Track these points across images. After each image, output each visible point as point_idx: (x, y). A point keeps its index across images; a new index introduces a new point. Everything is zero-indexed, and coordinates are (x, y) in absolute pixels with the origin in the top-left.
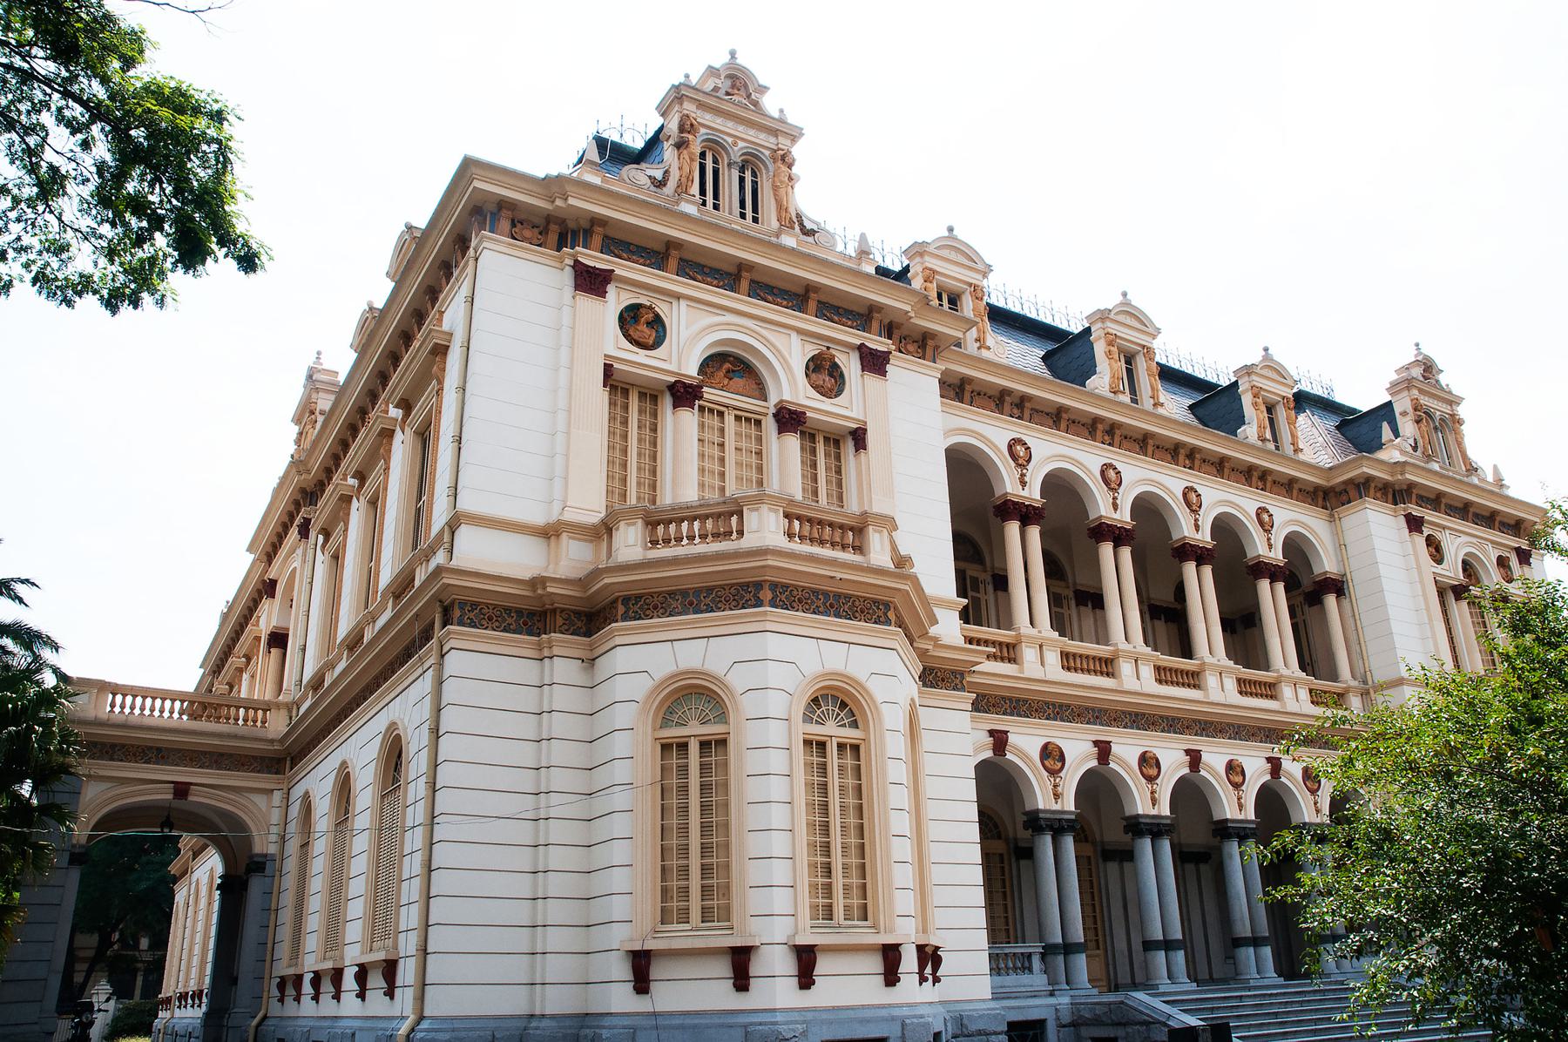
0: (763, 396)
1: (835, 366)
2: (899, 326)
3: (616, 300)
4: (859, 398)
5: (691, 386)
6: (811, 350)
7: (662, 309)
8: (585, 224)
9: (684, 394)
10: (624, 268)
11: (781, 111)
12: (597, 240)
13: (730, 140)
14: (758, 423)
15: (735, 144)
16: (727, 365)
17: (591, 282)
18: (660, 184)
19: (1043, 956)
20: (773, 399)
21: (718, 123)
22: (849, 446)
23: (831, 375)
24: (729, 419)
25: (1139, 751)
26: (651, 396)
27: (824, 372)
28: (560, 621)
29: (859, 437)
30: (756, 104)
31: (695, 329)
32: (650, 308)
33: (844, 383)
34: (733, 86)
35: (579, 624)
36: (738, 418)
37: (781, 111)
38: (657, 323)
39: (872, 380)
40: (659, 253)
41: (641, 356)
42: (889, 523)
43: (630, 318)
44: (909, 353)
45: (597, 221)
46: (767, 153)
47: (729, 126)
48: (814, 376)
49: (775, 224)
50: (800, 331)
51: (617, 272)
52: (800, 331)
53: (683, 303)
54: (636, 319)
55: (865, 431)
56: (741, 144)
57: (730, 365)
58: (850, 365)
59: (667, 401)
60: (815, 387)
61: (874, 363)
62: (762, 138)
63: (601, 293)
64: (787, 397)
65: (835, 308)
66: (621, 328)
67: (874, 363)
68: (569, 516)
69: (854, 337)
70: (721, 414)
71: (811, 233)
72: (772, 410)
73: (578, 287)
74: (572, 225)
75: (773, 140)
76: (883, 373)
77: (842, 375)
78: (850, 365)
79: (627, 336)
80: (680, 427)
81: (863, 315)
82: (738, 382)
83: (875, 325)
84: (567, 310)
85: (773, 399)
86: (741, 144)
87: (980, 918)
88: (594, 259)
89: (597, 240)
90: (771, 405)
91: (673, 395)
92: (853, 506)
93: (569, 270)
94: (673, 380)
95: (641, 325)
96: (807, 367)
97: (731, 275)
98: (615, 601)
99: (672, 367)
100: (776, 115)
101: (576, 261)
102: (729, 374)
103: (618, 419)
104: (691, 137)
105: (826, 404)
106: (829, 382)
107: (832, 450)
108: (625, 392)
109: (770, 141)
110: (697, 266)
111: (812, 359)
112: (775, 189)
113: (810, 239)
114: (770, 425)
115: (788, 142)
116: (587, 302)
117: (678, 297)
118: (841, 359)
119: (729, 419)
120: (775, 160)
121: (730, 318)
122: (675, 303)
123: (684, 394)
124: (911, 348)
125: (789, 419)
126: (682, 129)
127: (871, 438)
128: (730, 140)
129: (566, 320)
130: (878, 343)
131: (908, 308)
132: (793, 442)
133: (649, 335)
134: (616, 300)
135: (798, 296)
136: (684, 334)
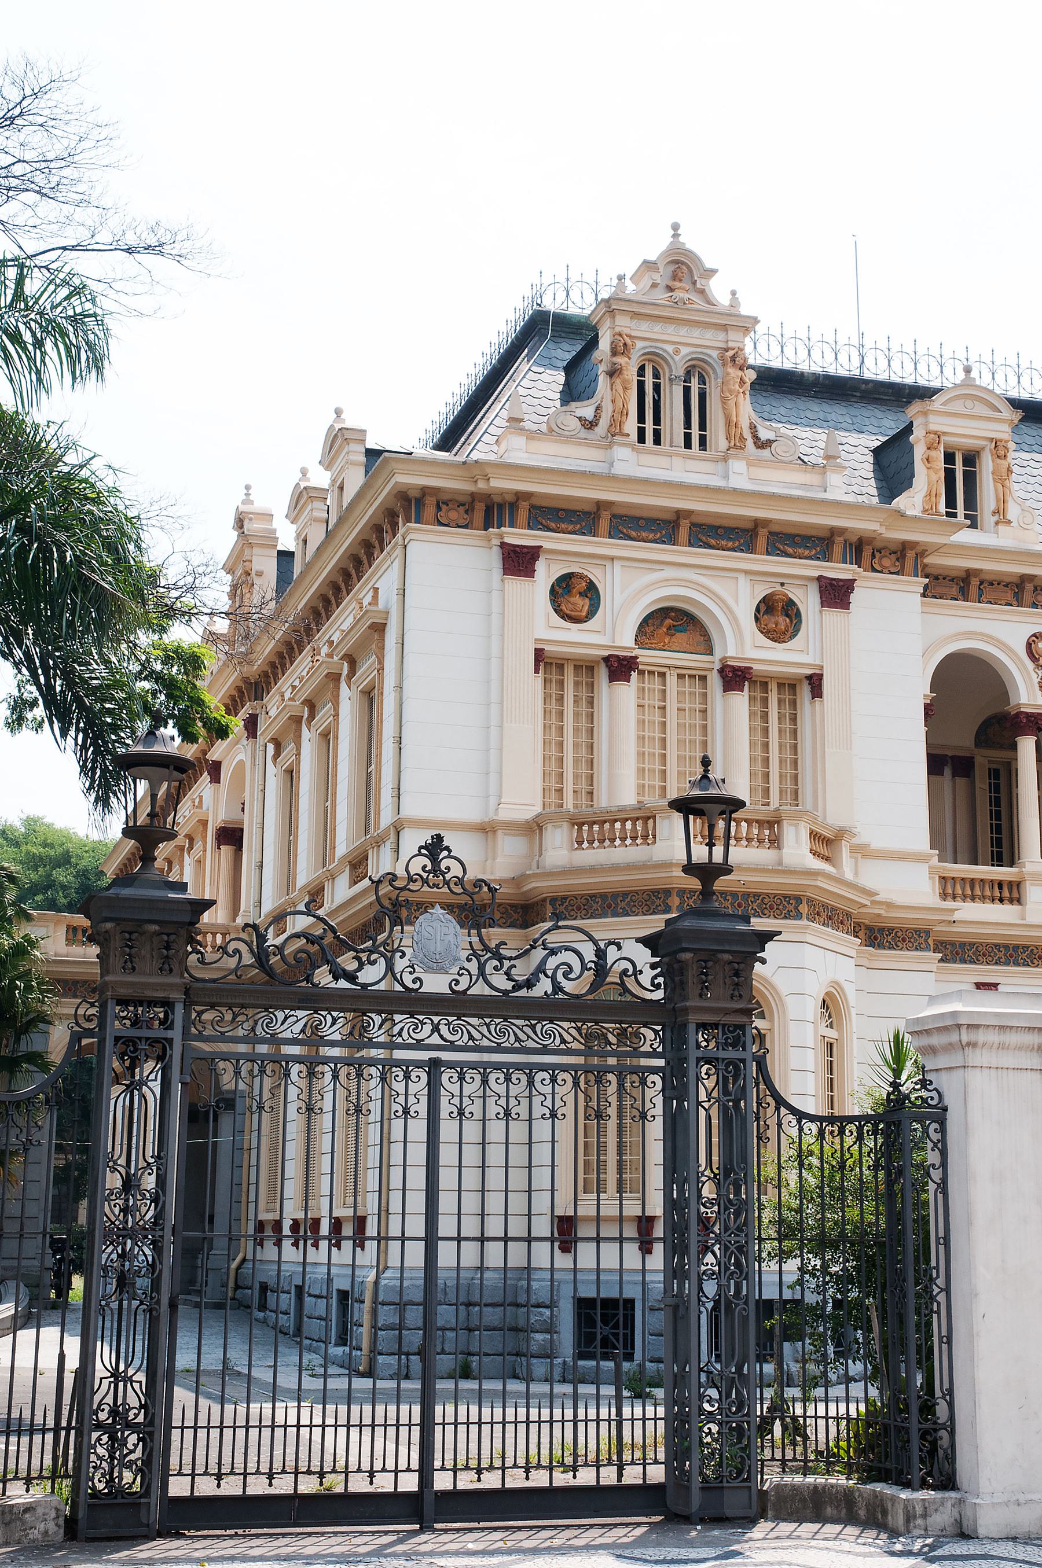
0: (711, 653)
4: (818, 639)
14: (703, 678)
15: (677, 352)
16: (669, 622)
17: (519, 562)
18: (590, 425)
20: (718, 654)
22: (805, 691)
24: (672, 679)
26: (585, 668)
28: (497, 916)
30: (702, 292)
33: (800, 621)
35: (516, 916)
36: (680, 676)
39: (833, 616)
50: (746, 572)
58: (808, 601)
60: (767, 633)
61: (836, 594)
64: (731, 652)
70: (662, 675)
72: (717, 666)
74: (497, 499)
75: (721, 336)
77: (798, 614)
80: (622, 700)
81: (819, 543)
82: (681, 638)
86: (684, 350)
91: (609, 667)
96: (758, 609)
98: (544, 900)
103: (554, 698)
106: (783, 621)
107: (787, 697)
108: (561, 667)
112: (724, 401)
113: (766, 453)
114: (715, 682)
117: (612, 559)
119: (672, 679)
122: (608, 564)
125: (735, 677)
126: (614, 353)
128: (670, 348)
136: (619, 599)
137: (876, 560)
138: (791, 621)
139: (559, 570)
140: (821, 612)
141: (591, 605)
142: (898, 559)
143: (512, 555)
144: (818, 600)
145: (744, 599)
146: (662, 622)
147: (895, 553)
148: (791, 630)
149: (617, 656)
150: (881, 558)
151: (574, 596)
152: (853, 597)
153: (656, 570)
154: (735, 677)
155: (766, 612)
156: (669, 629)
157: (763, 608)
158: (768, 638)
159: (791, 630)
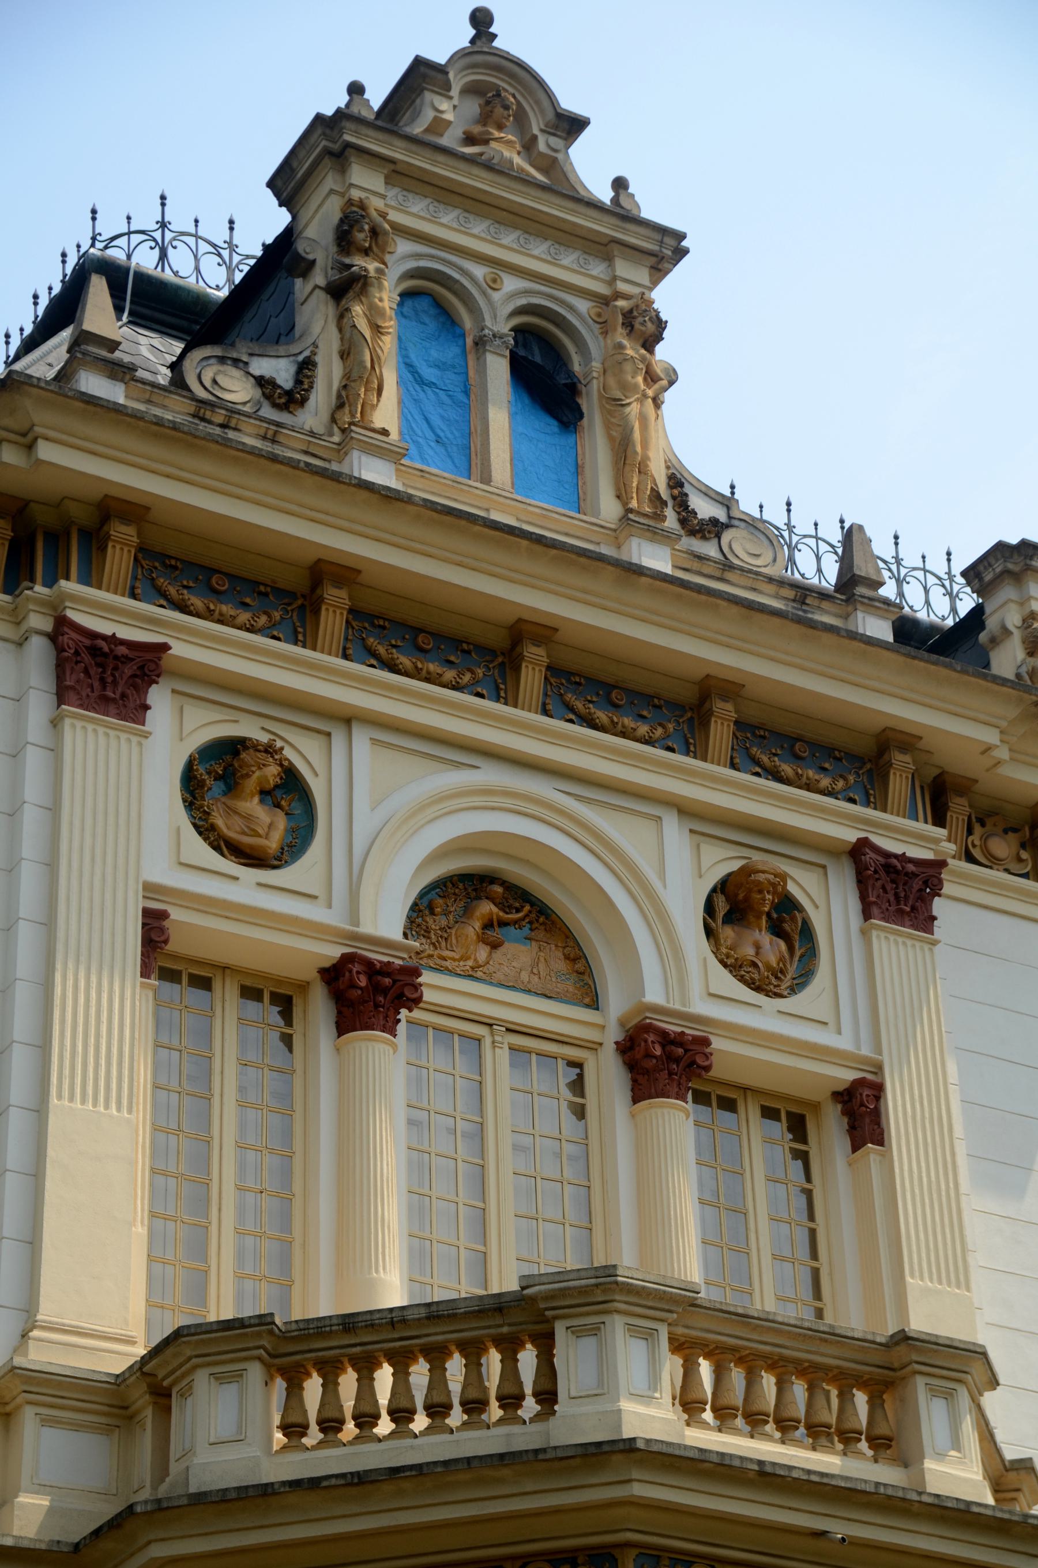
1: (788, 905)
2: (965, 787)
3: (173, 730)
5: (386, 970)
6: (721, 862)
7: (304, 752)
8: (81, 515)
9: (367, 993)
10: (197, 642)
11: (620, 184)
12: (119, 559)
13: (480, 272)
16: (487, 908)
20: (617, 1002)
21: (446, 225)
22: (830, 1132)
23: (777, 930)
27: (756, 920)
29: (861, 1110)
31: (395, 810)
32: (269, 750)
33: (811, 953)
34: (485, 118)
37: (620, 184)
38: (291, 790)
39: (893, 945)
40: (288, 596)
41: (245, 886)
42: (962, 1367)
43: (215, 776)
44: (993, 861)
45: (112, 509)
46: (583, 306)
47: (474, 235)
48: (728, 933)
49: (609, 509)
50: (685, 810)
51: (179, 649)
52: (685, 810)
53: (361, 738)
54: (231, 781)
55: (878, 1090)
56: (510, 284)
57: (488, 901)
58: (830, 903)
59: (318, 1011)
60: (734, 966)
61: (899, 893)
62: (571, 269)
63: (133, 710)
64: (654, 995)
65: (782, 742)
66: (190, 805)
67: (899, 893)
68: (40, 1356)
69: (838, 821)
71: (713, 529)
72: (613, 1035)
73: (62, 695)
76: (925, 922)
77: (807, 932)
78: (830, 903)
79: (206, 830)
81: (862, 761)
82: (518, 953)
83: (898, 785)
84: (34, 760)
85: (617, 1002)
88: (109, 610)
89: (119, 559)
90: (608, 1024)
92: (852, 1315)
93: (38, 648)
94: (334, 952)
95: (248, 797)
96: (709, 908)
97: (488, 655)
100: (605, 194)
101: (62, 623)
104: (372, 266)
105: (764, 1015)
106: (772, 949)
109: (591, 275)
110: (401, 632)
111: (723, 887)
114: (607, 1075)
115: (642, 275)
116: (90, 737)
117: (348, 719)
118: (804, 885)
119: (498, 1059)
120: (605, 328)
121: (490, 775)
123: (367, 993)
124: (1001, 847)
125: (664, 1061)
127: (898, 1107)
130: (907, 836)
131: (990, 736)
132: (676, 1121)
133: (271, 826)
134: (173, 730)
135: (680, 711)
136: (365, 823)
137: (976, 838)
138: (791, 949)
139: (207, 726)
140: (864, 933)
141: (292, 831)
142: (1023, 846)
143: (87, 658)
144: (854, 905)
145: (683, 873)
146: (468, 911)
147: (1015, 830)
148: (792, 970)
149: (368, 963)
150: (985, 838)
151: (248, 797)
152: (939, 906)
153: (459, 765)
154: (664, 1061)
155: (728, 919)
156: (488, 925)
157: (722, 906)
158: (742, 979)
159: (792, 970)
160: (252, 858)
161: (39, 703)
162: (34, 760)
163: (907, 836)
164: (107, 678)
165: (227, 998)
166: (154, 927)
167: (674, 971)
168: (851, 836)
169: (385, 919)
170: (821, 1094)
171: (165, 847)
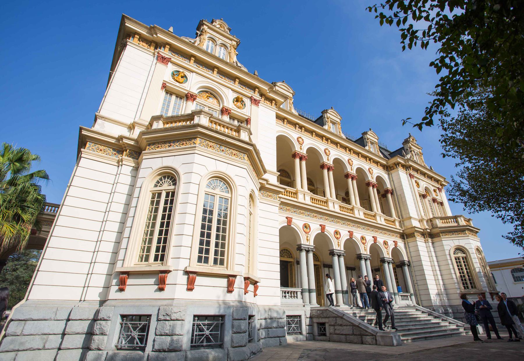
6: (236, 95)
7: (187, 73)
10: (176, 59)
19: (302, 293)
25: (334, 229)
40: (188, 56)
48: (236, 103)
67: (255, 102)
69: (249, 93)
78: (247, 101)
79: (174, 79)
84: (153, 67)
87: (278, 276)
99: (188, 89)
102: (208, 97)
118: (245, 99)
129: (152, 69)
134: (171, 68)
160: (180, 83)
161: (155, 61)
162: (153, 67)
163: (257, 96)
164: (164, 60)
165: (174, 97)
166: (164, 86)
167: (229, 103)
168: (250, 96)
169: (195, 91)
170: (244, 120)
171: (169, 78)
